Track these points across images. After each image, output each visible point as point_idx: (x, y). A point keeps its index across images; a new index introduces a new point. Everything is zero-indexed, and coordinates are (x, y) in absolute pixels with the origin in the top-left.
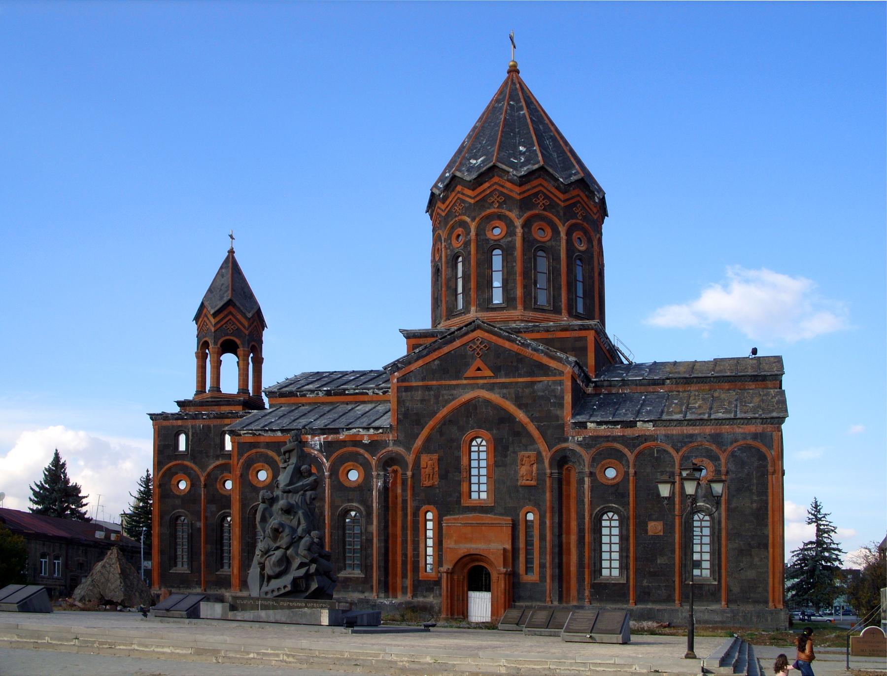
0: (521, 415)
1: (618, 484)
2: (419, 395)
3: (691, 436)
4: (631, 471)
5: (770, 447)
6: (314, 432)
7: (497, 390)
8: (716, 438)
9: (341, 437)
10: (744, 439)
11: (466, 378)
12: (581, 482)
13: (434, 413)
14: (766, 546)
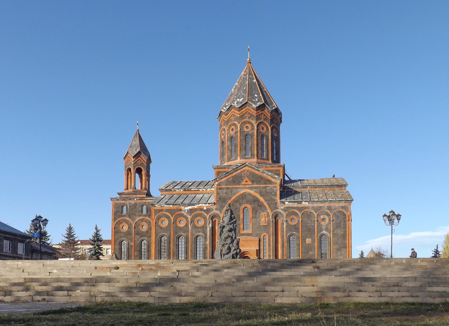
0: (262, 199)
2: (225, 191)
3: (321, 207)
4: (300, 220)
5: (347, 211)
6: (185, 205)
7: (253, 189)
8: (329, 208)
9: (196, 207)
10: (339, 208)
11: (242, 185)
12: (283, 224)
13: (230, 198)
14: (346, 247)
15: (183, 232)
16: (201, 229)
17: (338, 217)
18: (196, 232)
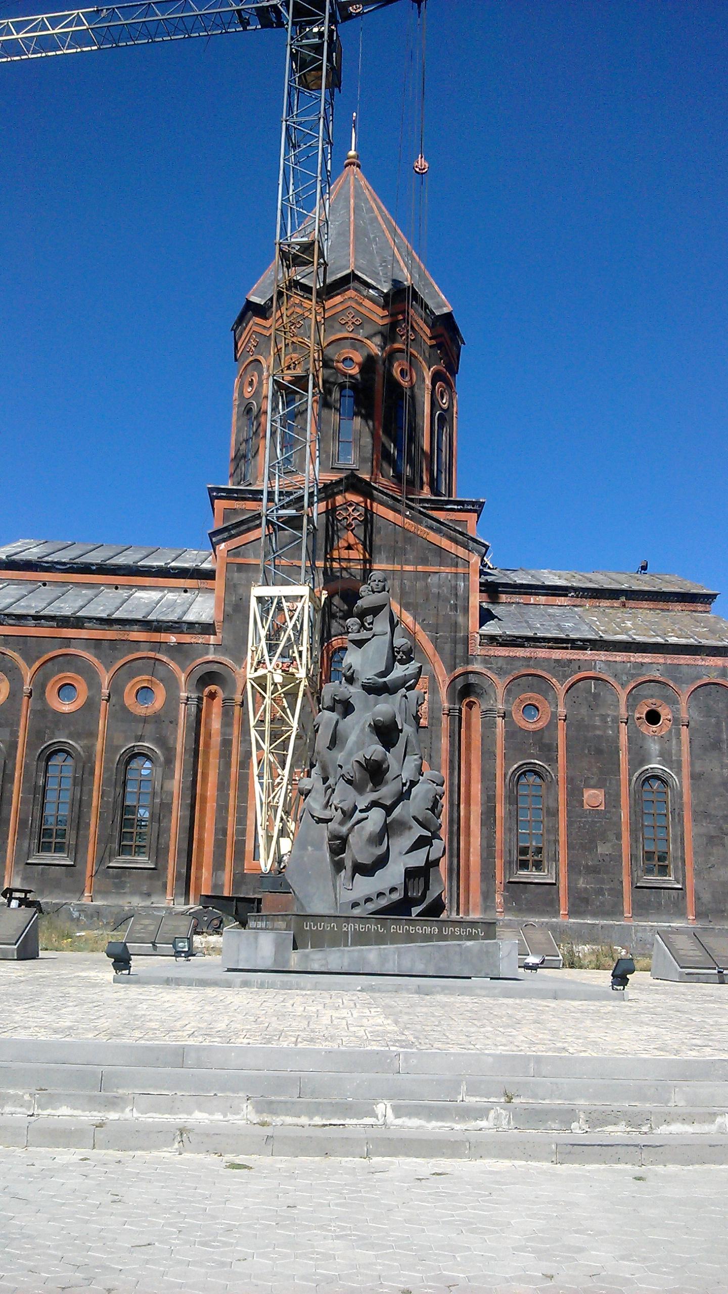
1: (542, 730)
4: (562, 711)
15: (70, 736)
16: (150, 728)
17: (708, 712)
18: (127, 740)
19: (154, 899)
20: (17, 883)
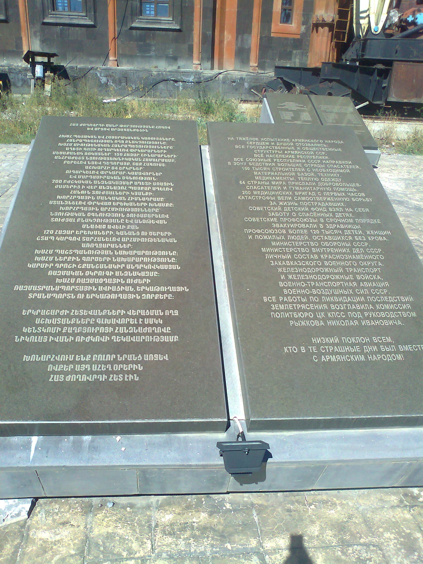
19: (181, 63)
20: (37, 47)
